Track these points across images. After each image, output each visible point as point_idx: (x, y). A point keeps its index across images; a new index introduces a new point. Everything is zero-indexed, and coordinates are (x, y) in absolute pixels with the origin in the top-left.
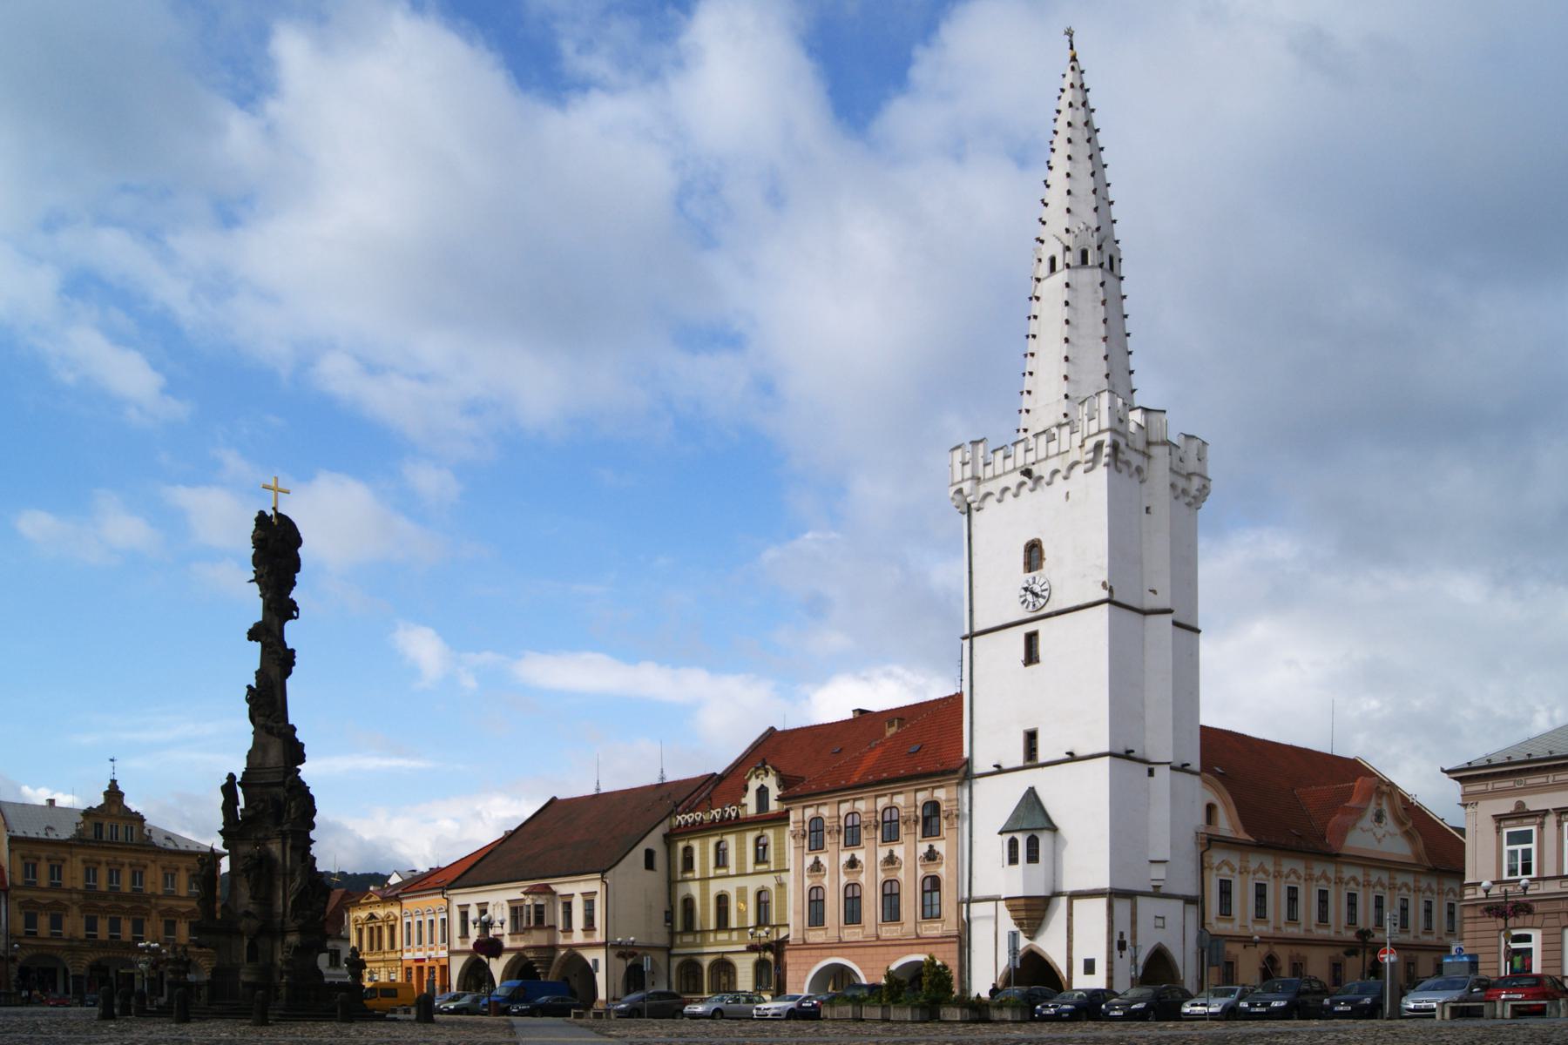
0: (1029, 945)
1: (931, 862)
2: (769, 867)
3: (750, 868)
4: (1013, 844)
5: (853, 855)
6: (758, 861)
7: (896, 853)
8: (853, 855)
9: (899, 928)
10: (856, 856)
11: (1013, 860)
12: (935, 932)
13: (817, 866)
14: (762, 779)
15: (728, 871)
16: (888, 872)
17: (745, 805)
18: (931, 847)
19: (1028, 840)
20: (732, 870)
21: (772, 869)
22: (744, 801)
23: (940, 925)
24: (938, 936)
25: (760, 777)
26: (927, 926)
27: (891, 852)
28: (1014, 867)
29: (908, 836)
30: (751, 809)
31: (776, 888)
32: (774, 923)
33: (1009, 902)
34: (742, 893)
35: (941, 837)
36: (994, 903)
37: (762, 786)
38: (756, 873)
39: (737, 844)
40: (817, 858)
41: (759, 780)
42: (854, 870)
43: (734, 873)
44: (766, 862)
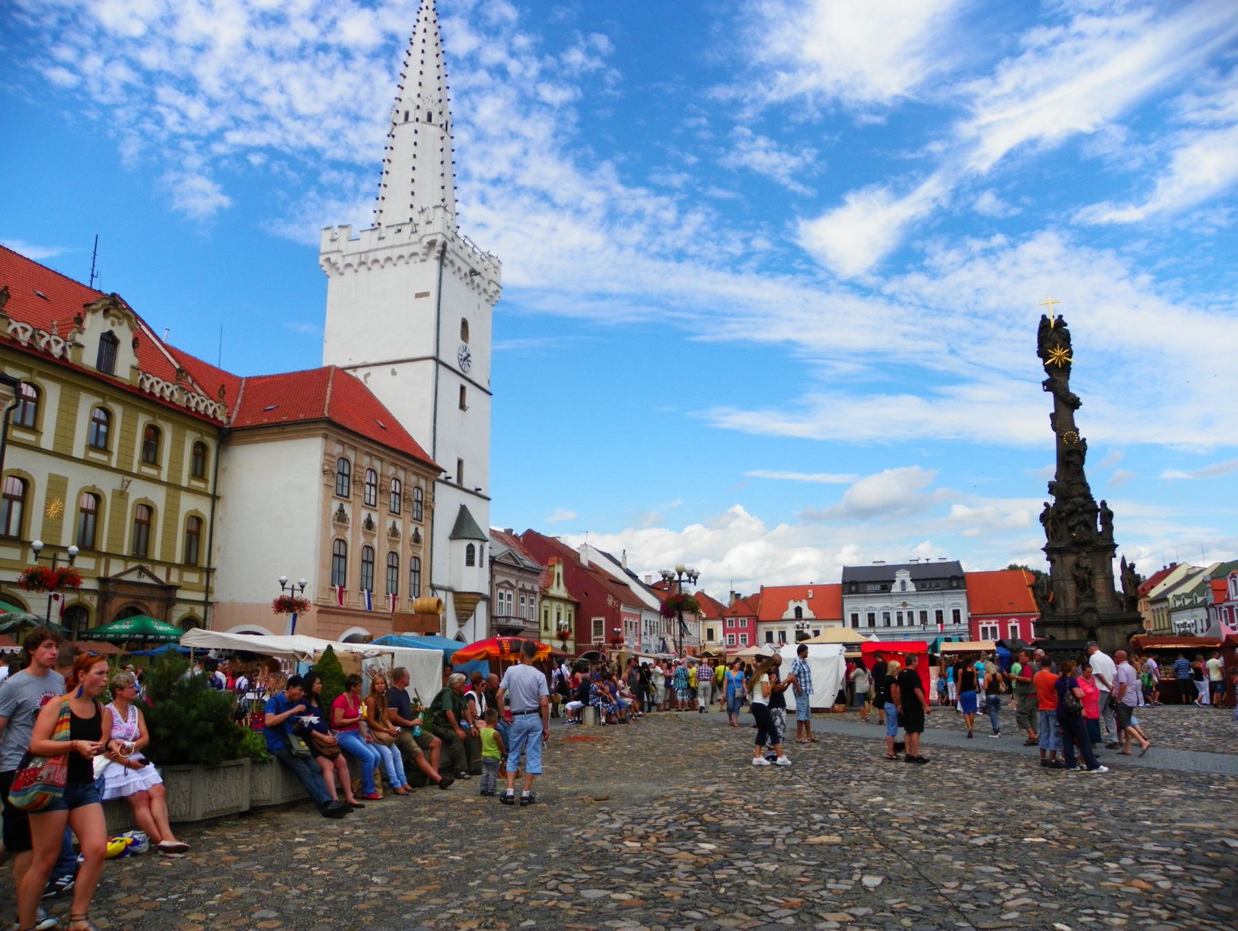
2: (110, 460)
3: (79, 451)
4: (470, 549)
6: (93, 447)
7: (397, 527)
11: (470, 562)
13: (341, 516)
14: (113, 324)
15: (38, 440)
17: (80, 346)
19: (468, 547)
20: (47, 440)
21: (114, 464)
22: (79, 338)
25: (111, 318)
30: (89, 358)
31: (113, 496)
32: (104, 550)
34: (57, 486)
37: (110, 333)
38: (85, 462)
39: (61, 402)
41: (109, 322)
43: (50, 448)
44: (106, 450)
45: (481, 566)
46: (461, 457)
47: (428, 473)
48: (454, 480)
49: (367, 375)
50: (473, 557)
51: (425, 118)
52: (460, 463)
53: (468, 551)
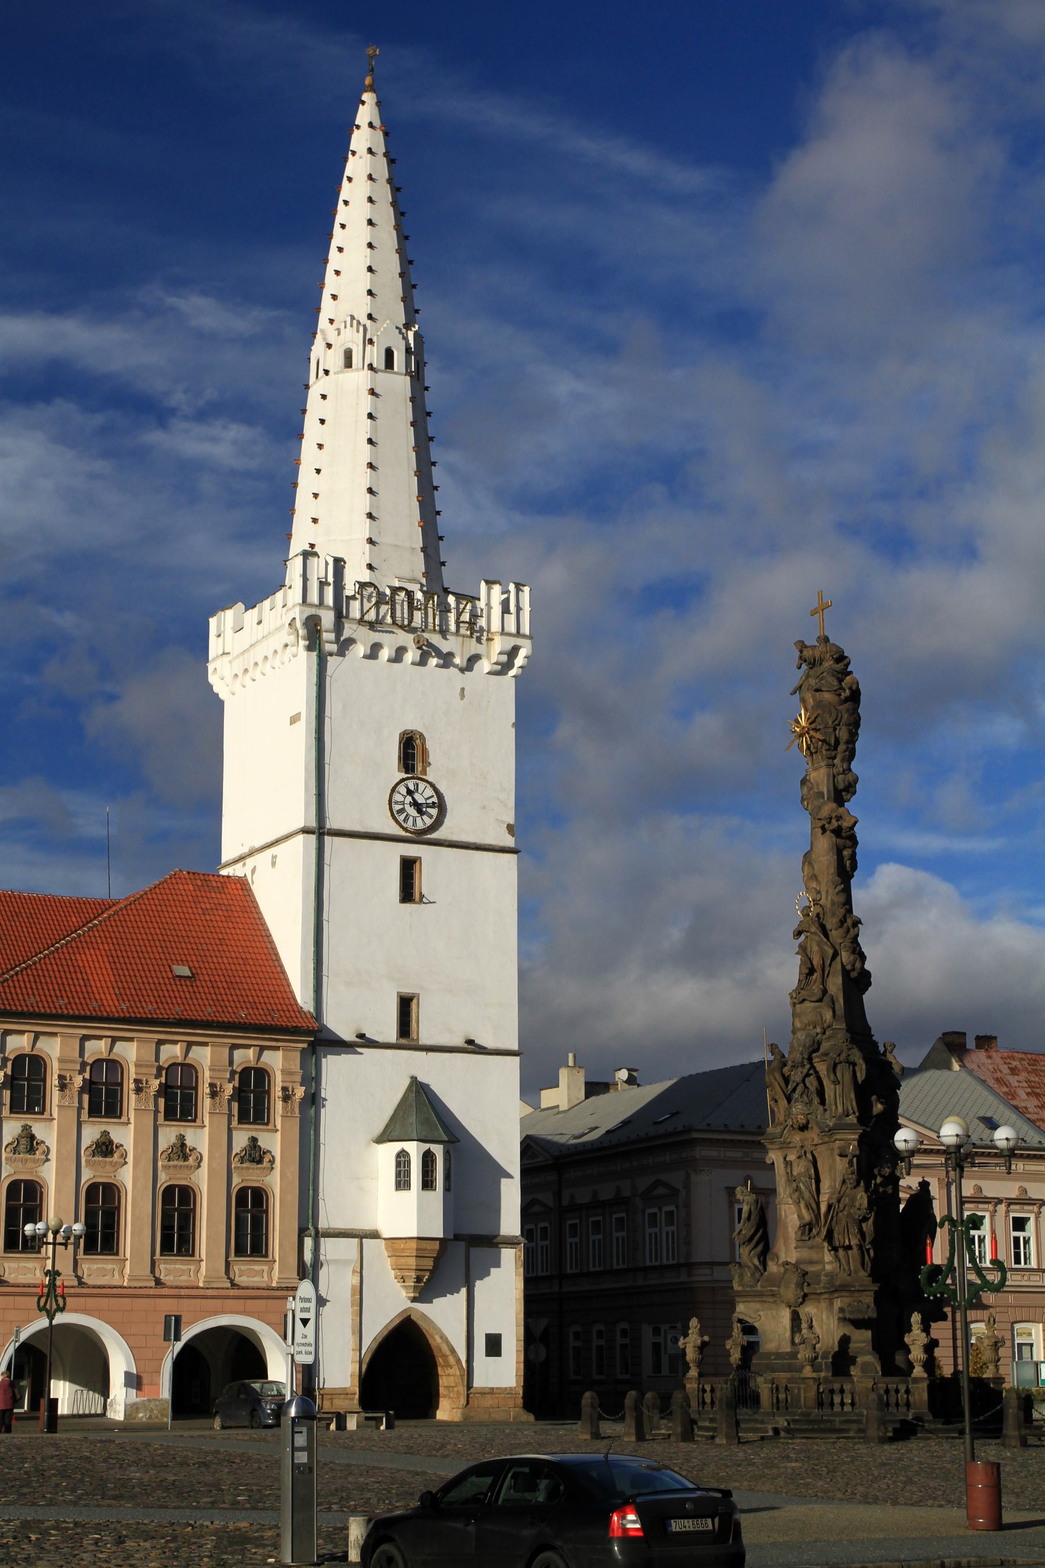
0: (409, 1308)
1: (254, 1165)
5: (105, 1134)
7: (189, 1142)
8: (105, 1134)
9: (192, 1268)
10: (113, 1136)
12: (256, 1279)
16: (171, 1171)
18: (254, 1140)
23: (266, 1268)
24: (264, 1285)
26: (243, 1268)
27: (181, 1138)
28: (403, 1193)
29: (216, 1118)
33: (389, 1242)
35: (271, 1127)
36: (356, 1240)
40: (26, 1128)
42: (107, 1159)
45: (427, 1184)
46: (407, 990)
47: (277, 1040)
48: (390, 1033)
49: (253, 871)
50: (408, 1173)
51: (341, 360)
52: (405, 1004)
53: (398, 1164)
